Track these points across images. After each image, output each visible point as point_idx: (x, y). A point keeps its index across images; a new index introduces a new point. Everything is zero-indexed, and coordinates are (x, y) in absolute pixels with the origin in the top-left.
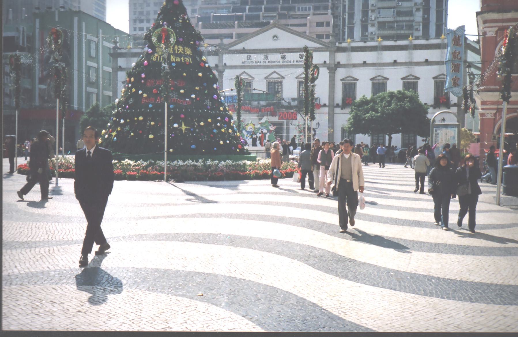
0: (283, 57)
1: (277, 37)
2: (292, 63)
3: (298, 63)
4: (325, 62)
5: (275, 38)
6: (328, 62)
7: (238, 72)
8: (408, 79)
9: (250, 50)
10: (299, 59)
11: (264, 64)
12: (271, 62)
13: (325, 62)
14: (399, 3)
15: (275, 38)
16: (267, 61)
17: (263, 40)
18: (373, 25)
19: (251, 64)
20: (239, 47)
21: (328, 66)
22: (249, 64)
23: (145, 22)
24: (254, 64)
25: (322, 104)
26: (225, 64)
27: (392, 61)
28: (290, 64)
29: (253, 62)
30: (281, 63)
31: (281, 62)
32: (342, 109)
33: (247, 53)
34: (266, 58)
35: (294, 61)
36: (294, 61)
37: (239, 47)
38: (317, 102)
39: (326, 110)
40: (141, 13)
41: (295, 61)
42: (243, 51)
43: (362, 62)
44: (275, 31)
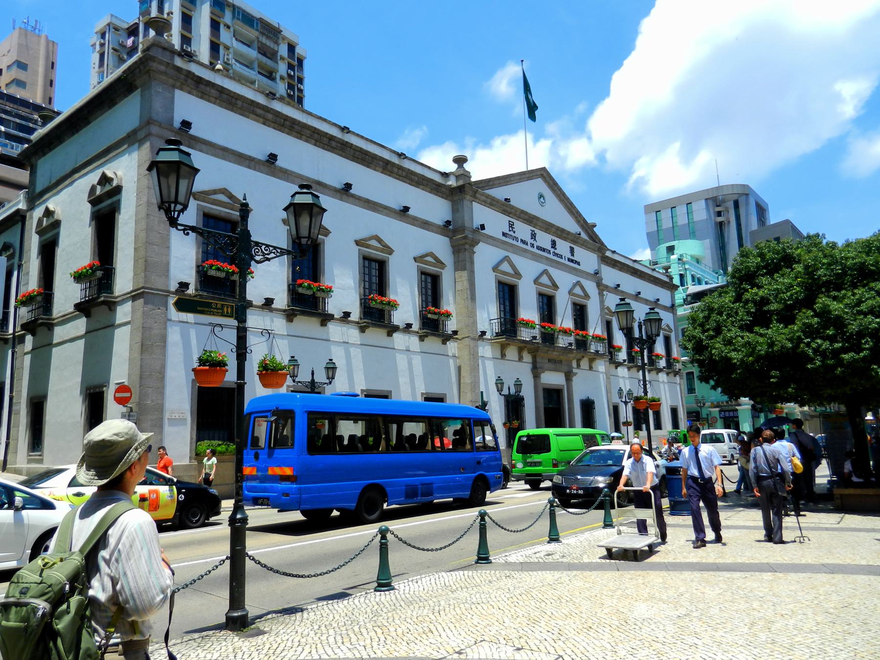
0: (554, 244)
2: (562, 261)
15: (542, 199)
19: (514, 242)
24: (519, 244)
26: (483, 227)
29: (516, 239)
30: (551, 256)
42: (505, 207)
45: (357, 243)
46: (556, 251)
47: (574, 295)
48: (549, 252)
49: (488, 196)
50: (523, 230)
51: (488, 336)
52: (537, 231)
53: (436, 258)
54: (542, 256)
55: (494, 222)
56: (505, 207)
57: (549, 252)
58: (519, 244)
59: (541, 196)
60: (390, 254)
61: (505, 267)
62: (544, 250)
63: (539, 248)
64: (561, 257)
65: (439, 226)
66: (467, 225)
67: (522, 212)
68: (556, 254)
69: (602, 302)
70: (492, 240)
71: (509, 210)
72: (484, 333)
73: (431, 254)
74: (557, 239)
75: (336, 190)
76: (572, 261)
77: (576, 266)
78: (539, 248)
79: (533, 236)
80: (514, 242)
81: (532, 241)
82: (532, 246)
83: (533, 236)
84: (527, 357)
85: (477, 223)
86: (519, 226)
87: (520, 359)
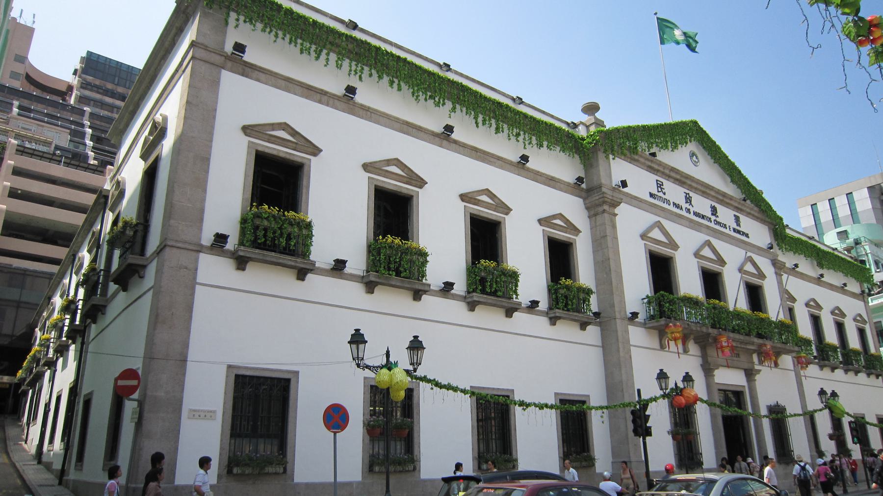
0: (714, 211)
1: (697, 158)
2: (727, 231)
5: (694, 158)
11: (687, 215)
15: (694, 158)
19: (665, 206)
24: (672, 208)
26: (624, 184)
29: (668, 202)
30: (712, 225)
45: (464, 197)
46: (718, 220)
47: (747, 273)
48: (710, 220)
50: (675, 193)
51: (641, 318)
53: (567, 221)
54: (701, 225)
55: (639, 181)
57: (710, 220)
58: (672, 208)
59: (693, 154)
60: (507, 214)
61: (656, 234)
62: (703, 217)
63: (696, 214)
64: (725, 226)
65: (568, 184)
66: (604, 181)
67: (673, 169)
69: (780, 283)
70: (636, 201)
71: (656, 167)
72: (635, 315)
73: (560, 216)
74: (717, 206)
75: (435, 134)
76: (739, 232)
77: (744, 238)
78: (696, 214)
79: (688, 200)
80: (665, 206)
81: (687, 205)
82: (688, 211)
83: (688, 200)
84: (693, 348)
85: (616, 180)
86: (668, 185)
87: (686, 351)
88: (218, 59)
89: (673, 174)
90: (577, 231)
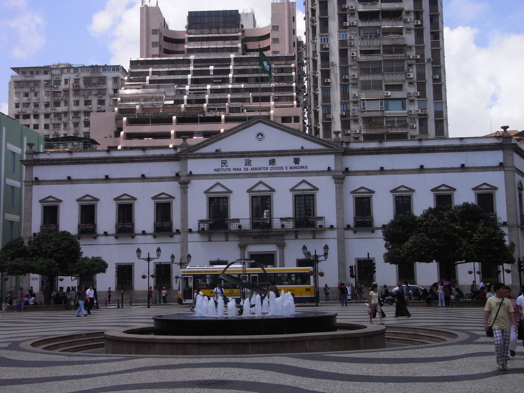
1: (262, 135)
2: (284, 170)
3: (292, 170)
4: (329, 168)
5: (260, 137)
6: (333, 168)
7: (207, 184)
8: (481, 189)
9: (225, 153)
10: (293, 165)
11: (246, 172)
12: (256, 169)
13: (329, 168)
14: (387, 93)
15: (260, 137)
16: (249, 167)
17: (245, 140)
18: (356, 121)
20: (211, 149)
21: (333, 174)
22: (224, 172)
23: (32, 117)
24: (232, 172)
25: (327, 225)
26: (191, 172)
27: (419, 167)
28: (281, 171)
29: (229, 169)
30: (269, 171)
31: (269, 168)
32: (355, 232)
33: (222, 157)
34: (248, 163)
35: (286, 168)
36: (286, 168)
37: (211, 149)
38: (319, 223)
39: (334, 234)
40: (27, 105)
41: (289, 168)
42: (217, 154)
43: (459, 166)
44: (260, 127)
49: (197, 154)
52: (251, 159)
53: (167, 195)
56: (217, 154)
65: (171, 177)
68: (276, 168)
74: (274, 158)
75: (103, 180)
81: (247, 167)
88: (30, 184)
89: (232, 155)
90: (173, 198)
